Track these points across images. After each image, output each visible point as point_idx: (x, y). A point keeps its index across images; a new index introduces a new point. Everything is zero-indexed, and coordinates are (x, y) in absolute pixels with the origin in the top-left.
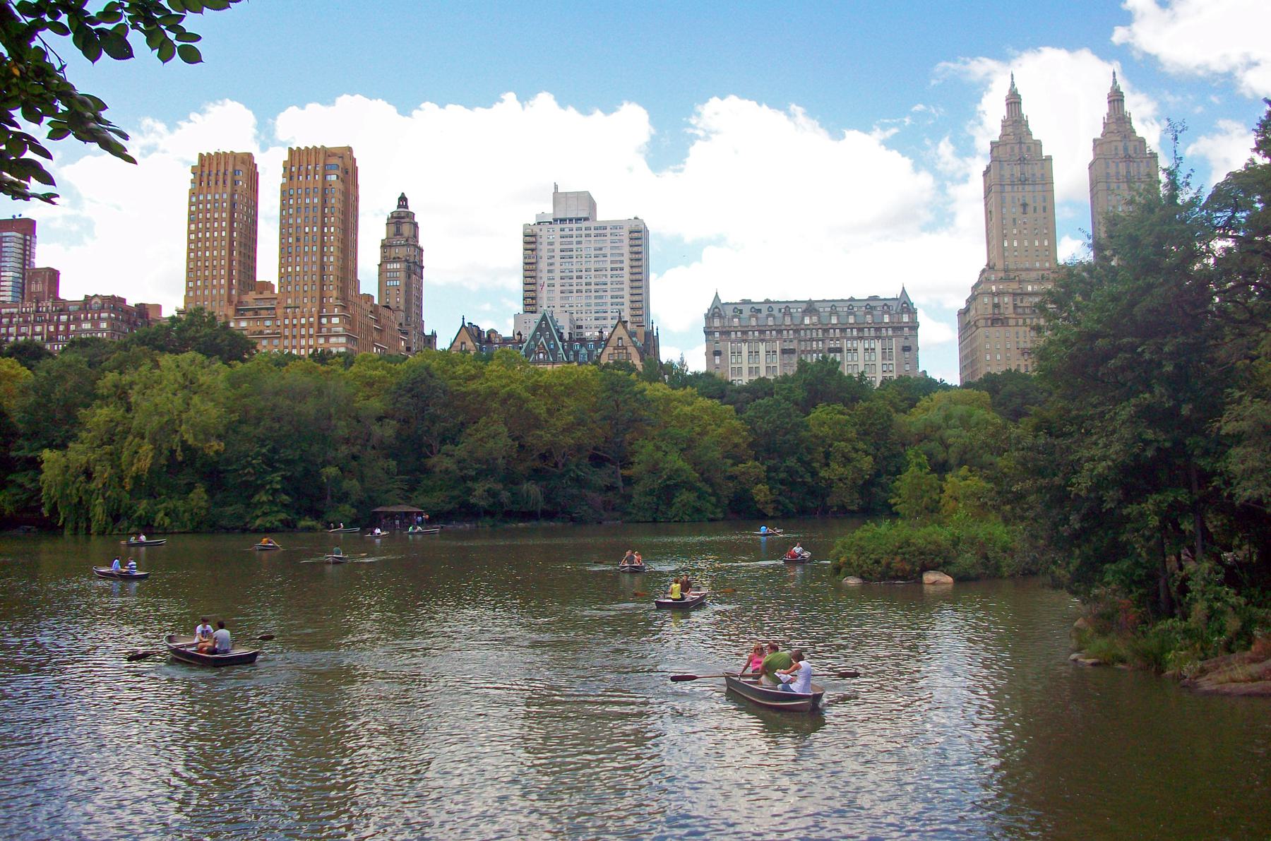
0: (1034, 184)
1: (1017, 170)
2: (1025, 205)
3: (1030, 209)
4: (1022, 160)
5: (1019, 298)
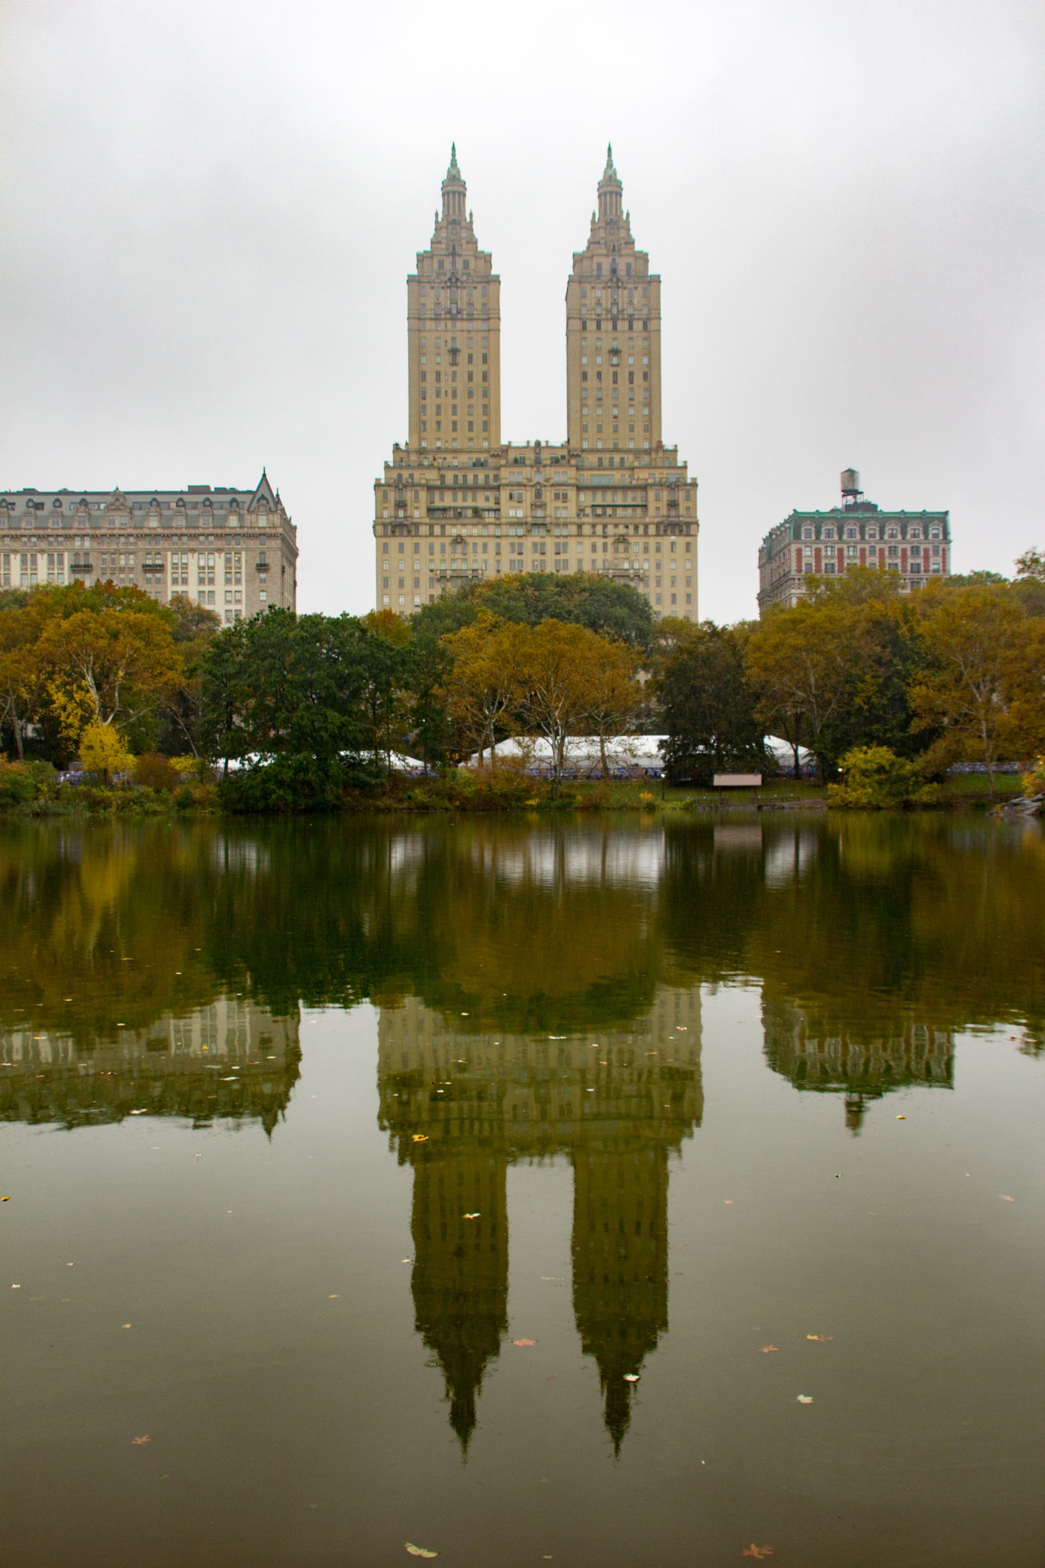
0: (471, 319)
1: (445, 296)
2: (454, 352)
3: (462, 358)
4: (453, 282)
5: (437, 494)
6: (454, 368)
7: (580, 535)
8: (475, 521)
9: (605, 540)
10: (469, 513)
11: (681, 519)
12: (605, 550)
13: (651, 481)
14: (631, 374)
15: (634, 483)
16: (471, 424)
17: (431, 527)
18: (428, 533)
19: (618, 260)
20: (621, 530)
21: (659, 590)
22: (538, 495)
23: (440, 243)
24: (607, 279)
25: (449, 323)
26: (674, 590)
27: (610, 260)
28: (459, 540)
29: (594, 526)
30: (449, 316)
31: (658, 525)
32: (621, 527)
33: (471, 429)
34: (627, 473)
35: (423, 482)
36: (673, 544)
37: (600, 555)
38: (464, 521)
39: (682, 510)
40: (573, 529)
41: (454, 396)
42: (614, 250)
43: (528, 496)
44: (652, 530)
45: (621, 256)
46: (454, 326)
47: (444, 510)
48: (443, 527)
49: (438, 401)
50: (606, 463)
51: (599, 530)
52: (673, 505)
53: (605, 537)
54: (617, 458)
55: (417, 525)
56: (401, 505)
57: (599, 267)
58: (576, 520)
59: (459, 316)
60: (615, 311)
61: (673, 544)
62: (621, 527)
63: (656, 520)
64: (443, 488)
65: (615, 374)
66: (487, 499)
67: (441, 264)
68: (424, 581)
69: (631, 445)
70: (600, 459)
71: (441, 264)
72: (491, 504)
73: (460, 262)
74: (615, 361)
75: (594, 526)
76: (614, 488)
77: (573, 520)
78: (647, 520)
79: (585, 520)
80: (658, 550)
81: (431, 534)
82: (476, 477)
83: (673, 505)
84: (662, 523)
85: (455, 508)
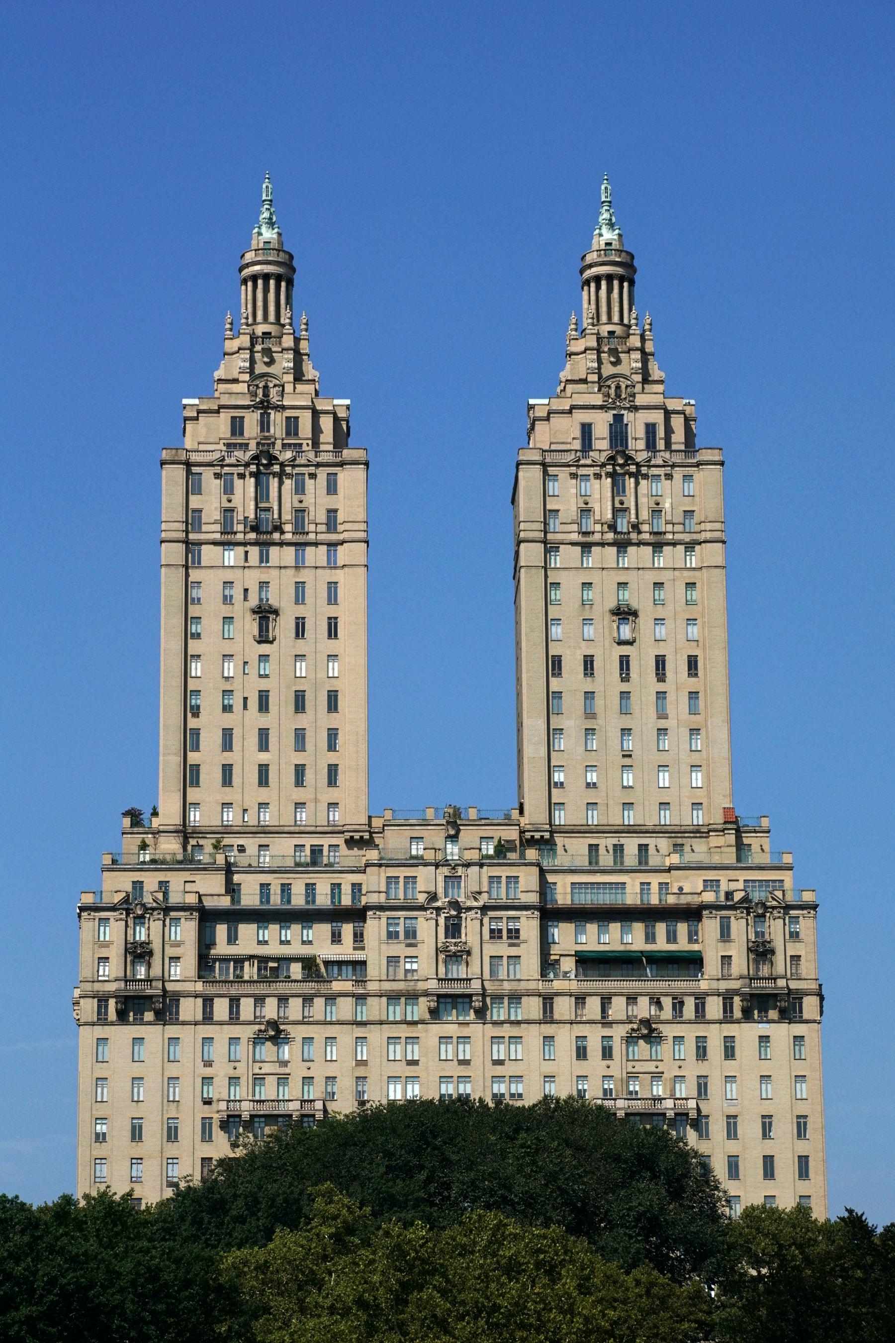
3: (283, 627)
6: (265, 648)
7: (548, 1018)
8: (309, 988)
9: (607, 1032)
10: (296, 970)
11: (781, 983)
12: (607, 1053)
13: (709, 897)
14: (660, 662)
15: (671, 900)
16: (300, 771)
17: (208, 1002)
18: (199, 1017)
19: (628, 417)
20: (643, 1009)
21: (733, 1147)
22: (453, 929)
23: (236, 381)
24: (603, 458)
25: (254, 551)
26: (768, 1148)
27: (609, 417)
29: (580, 999)
30: (253, 536)
31: (727, 998)
32: (644, 1001)
33: (299, 781)
34: (655, 880)
35: (192, 899)
36: (764, 1039)
37: (595, 1064)
38: (282, 988)
40: (532, 1007)
42: (618, 396)
44: (714, 1008)
45: (636, 408)
46: (264, 558)
47: (239, 961)
48: (235, 1002)
49: (228, 720)
50: (606, 859)
51: (593, 1006)
52: (761, 952)
53: (605, 1022)
56: (138, 953)
57: (586, 430)
58: (541, 986)
59: (276, 536)
60: (623, 525)
61: (764, 1039)
62: (644, 1001)
63: (723, 986)
64: (236, 916)
65: (625, 663)
66: (336, 938)
67: (237, 426)
68: (189, 1130)
69: (667, 818)
70: (594, 848)
71: (237, 426)
72: (346, 951)
73: (277, 419)
74: (626, 632)
75: (580, 999)
76: (625, 915)
77: (532, 985)
78: (704, 985)
79: (558, 985)
80: (730, 1052)
81: (208, 1018)
82: (310, 888)
84: (736, 992)
85: (263, 960)
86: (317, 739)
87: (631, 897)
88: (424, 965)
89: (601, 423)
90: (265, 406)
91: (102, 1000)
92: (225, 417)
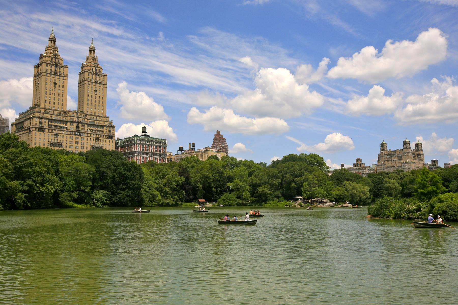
1: (53, 68)
3: (57, 86)
14: (99, 97)
20: (97, 136)
28: (56, 134)
39: (112, 133)
41: (54, 95)
43: (75, 125)
54: (95, 117)
55: (45, 129)
71: (52, 59)
83: (110, 131)
86: (61, 100)
87: (96, 124)
88: (74, 128)
89: (94, 68)
90: (56, 58)
91: (36, 128)
92: (50, 58)
